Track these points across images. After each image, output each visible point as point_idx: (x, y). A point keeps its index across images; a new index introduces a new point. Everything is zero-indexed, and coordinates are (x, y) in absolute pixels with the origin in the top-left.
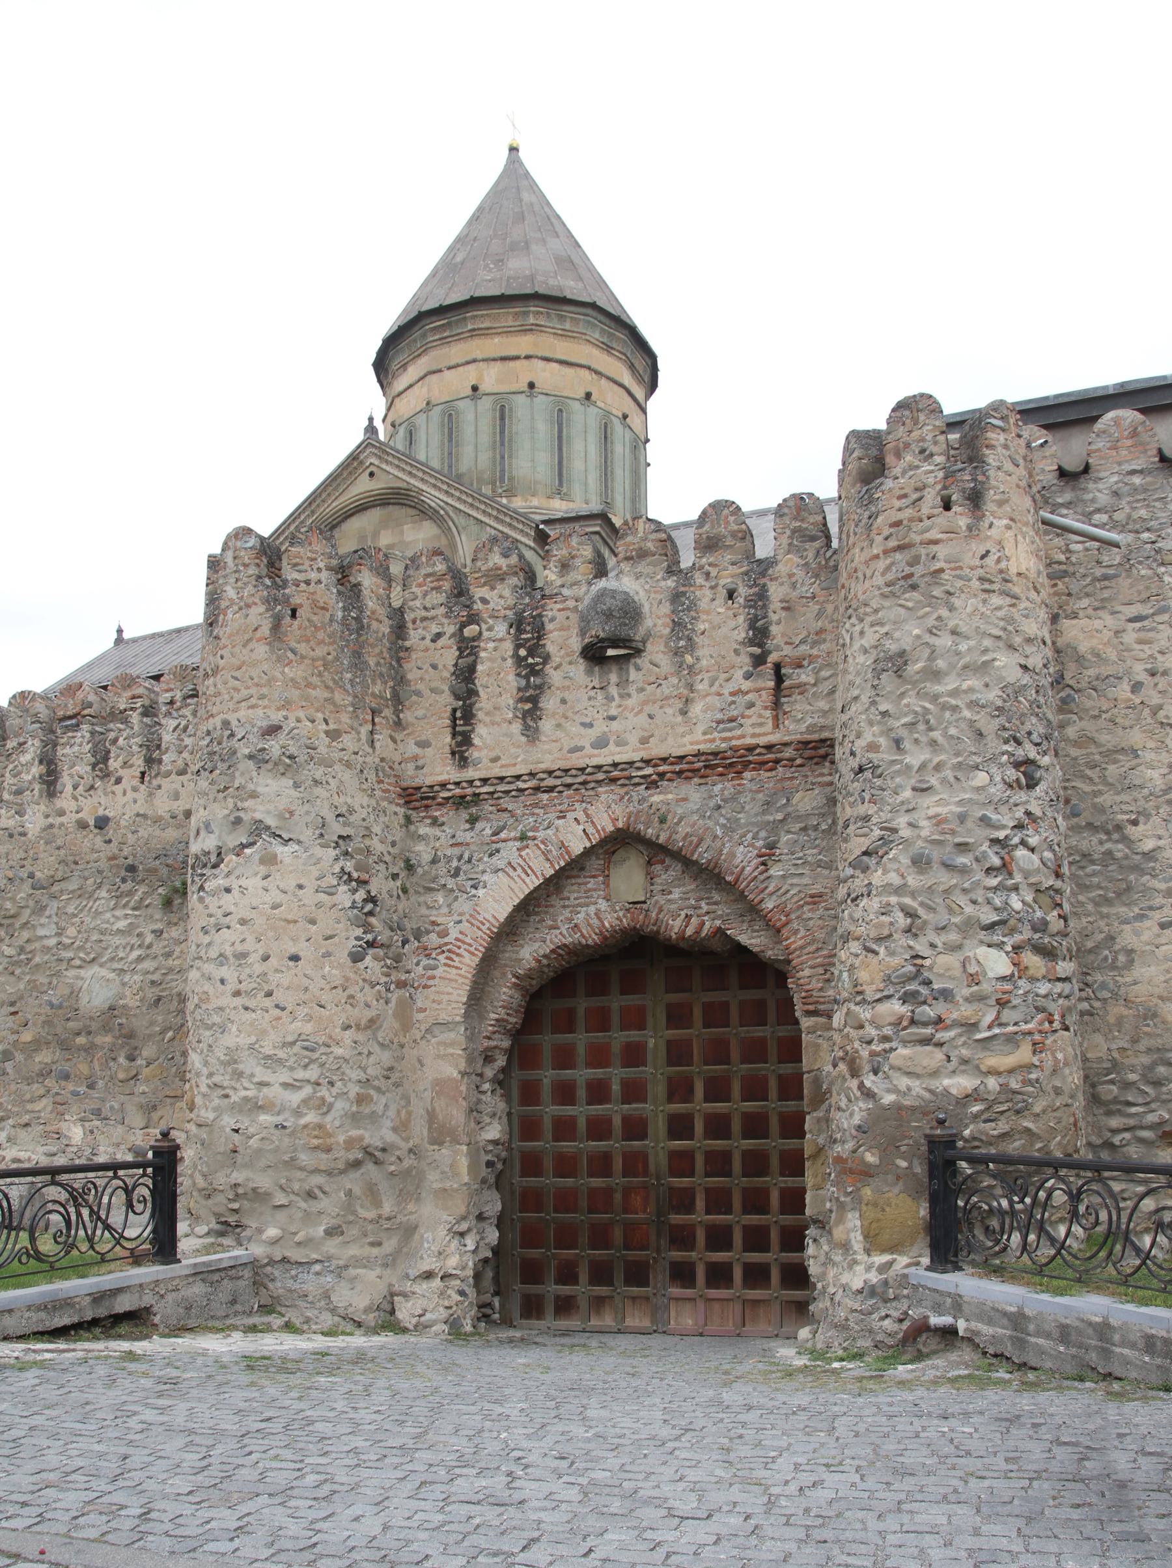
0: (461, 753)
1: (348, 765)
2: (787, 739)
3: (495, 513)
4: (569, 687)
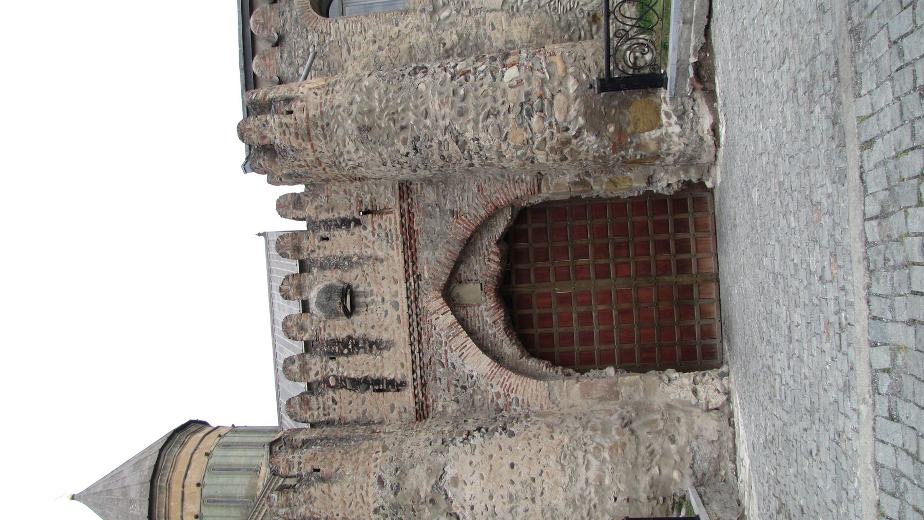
0: (398, 385)
1: (402, 441)
2: (398, 206)
4: (366, 325)
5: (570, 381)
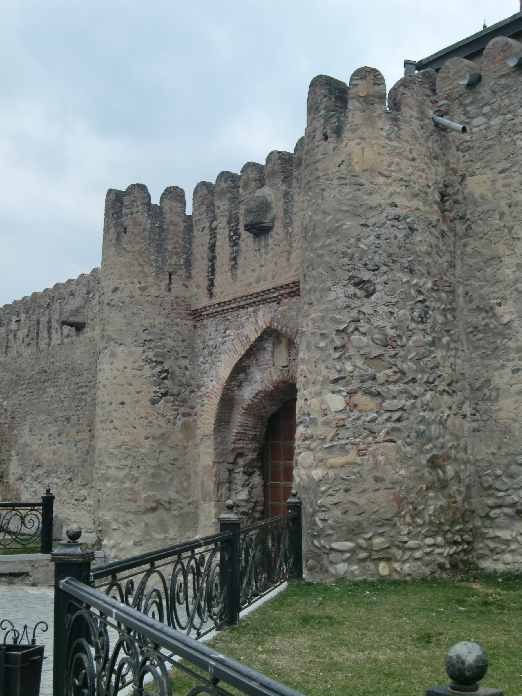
1: (152, 303)
5: (213, 455)
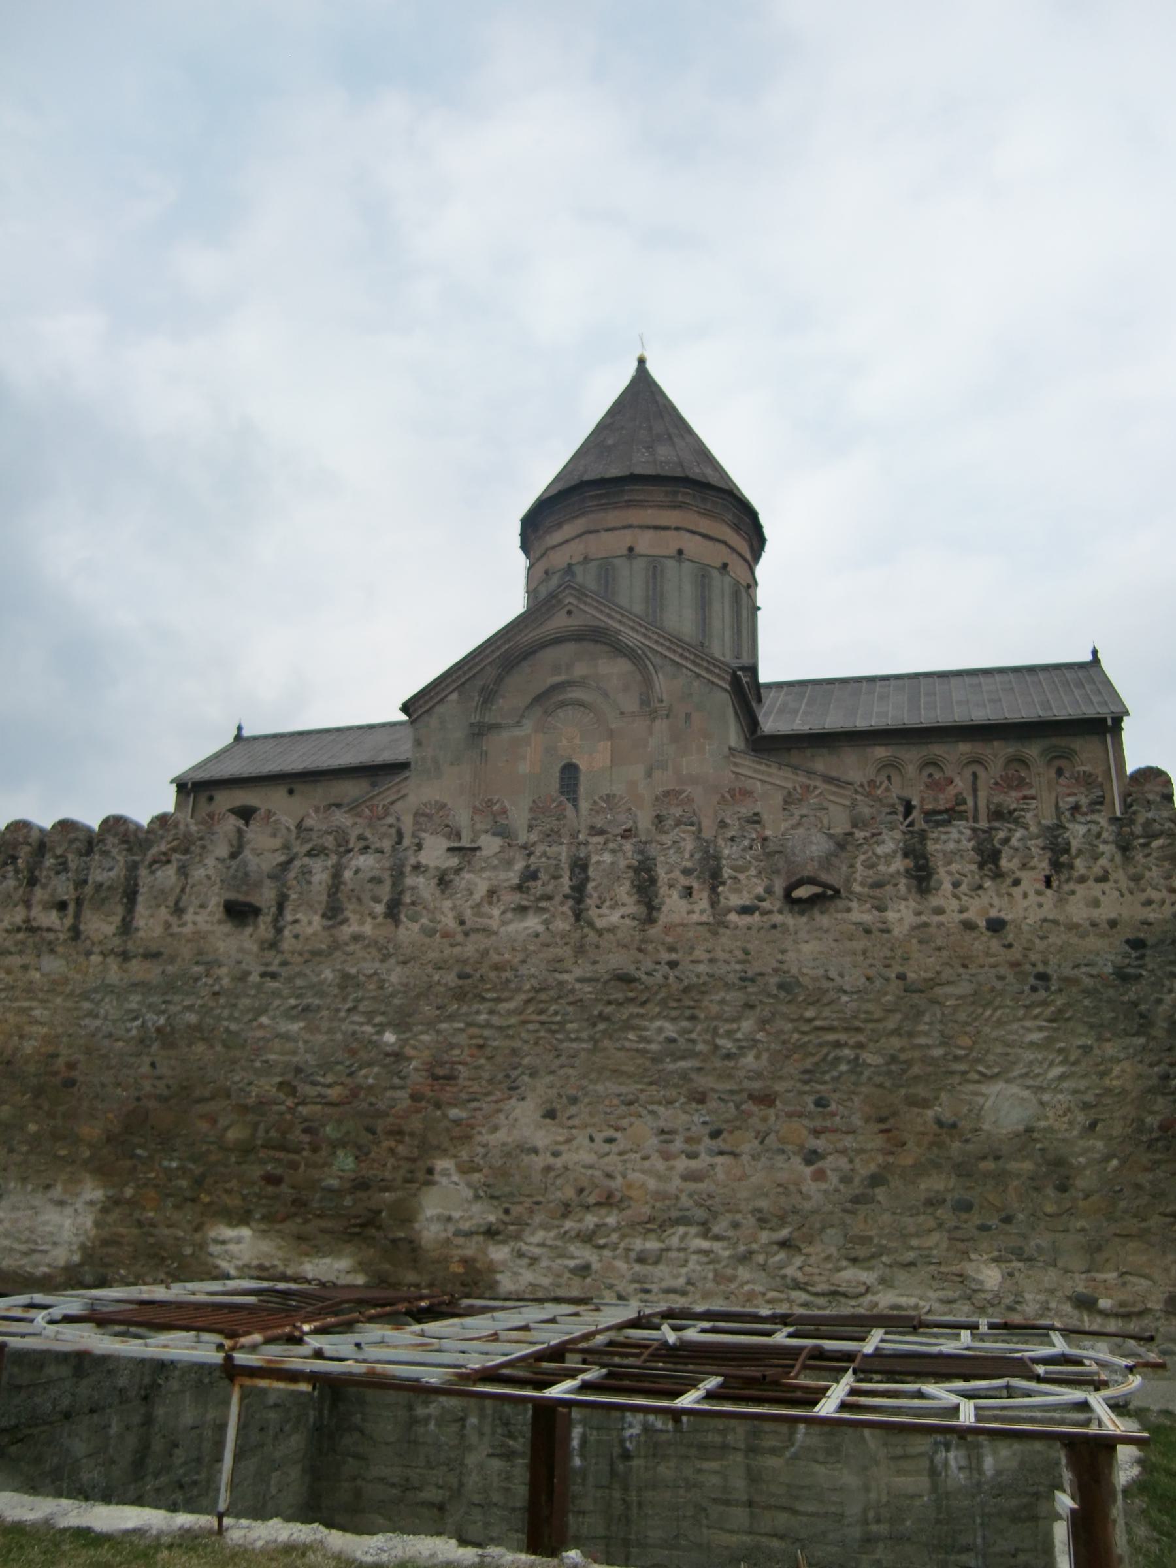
3: (692, 657)
